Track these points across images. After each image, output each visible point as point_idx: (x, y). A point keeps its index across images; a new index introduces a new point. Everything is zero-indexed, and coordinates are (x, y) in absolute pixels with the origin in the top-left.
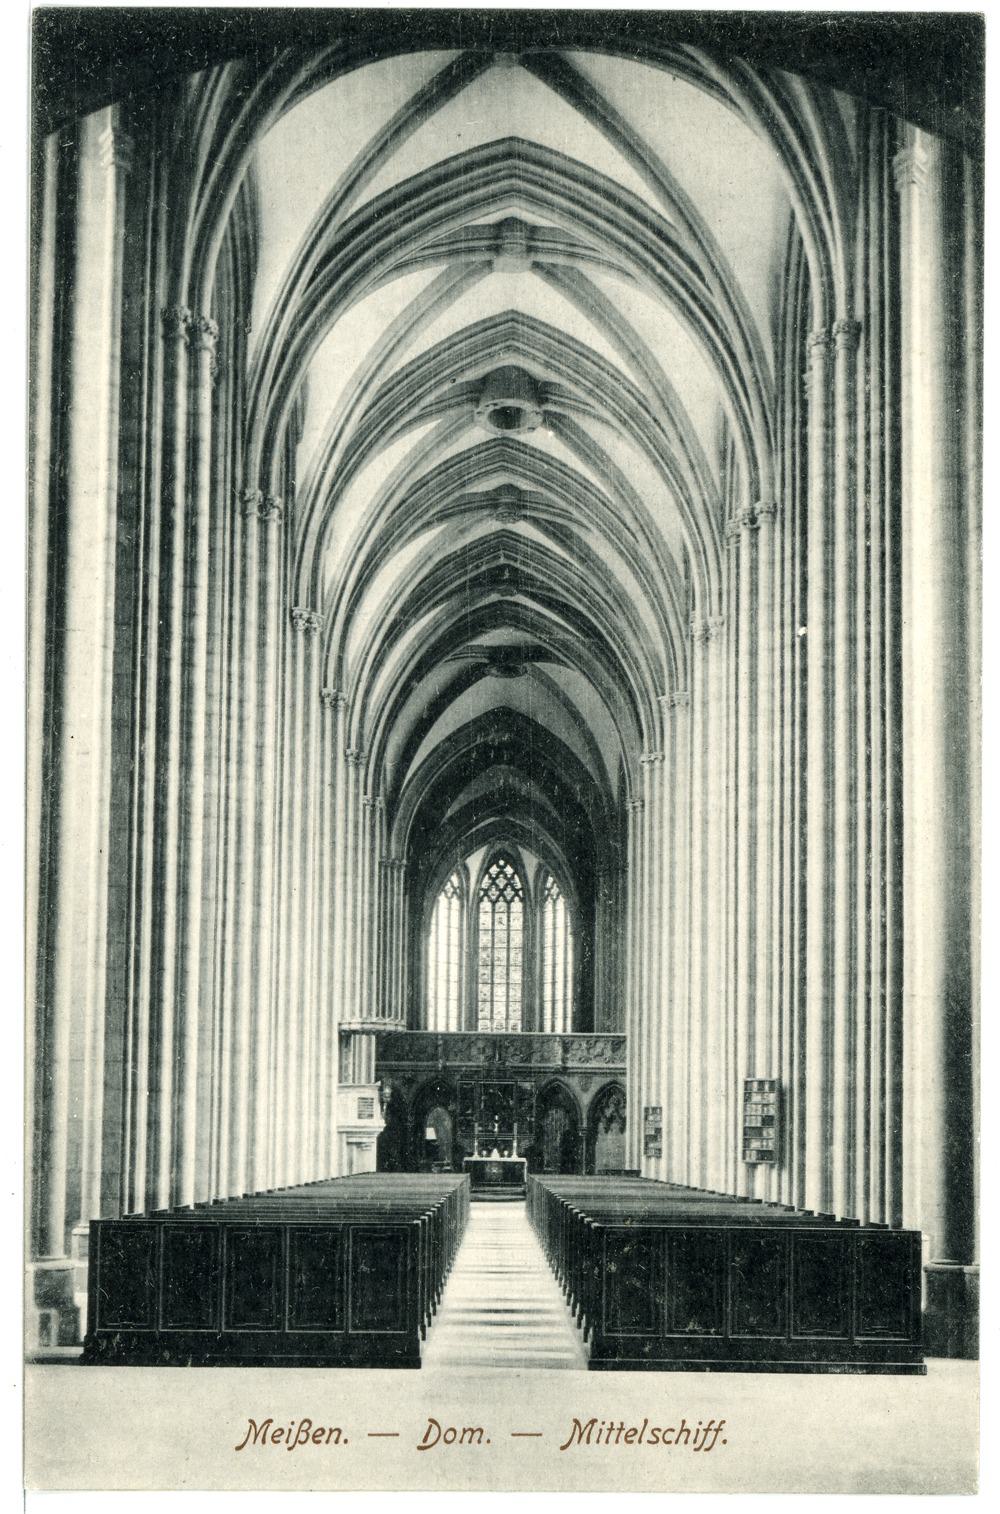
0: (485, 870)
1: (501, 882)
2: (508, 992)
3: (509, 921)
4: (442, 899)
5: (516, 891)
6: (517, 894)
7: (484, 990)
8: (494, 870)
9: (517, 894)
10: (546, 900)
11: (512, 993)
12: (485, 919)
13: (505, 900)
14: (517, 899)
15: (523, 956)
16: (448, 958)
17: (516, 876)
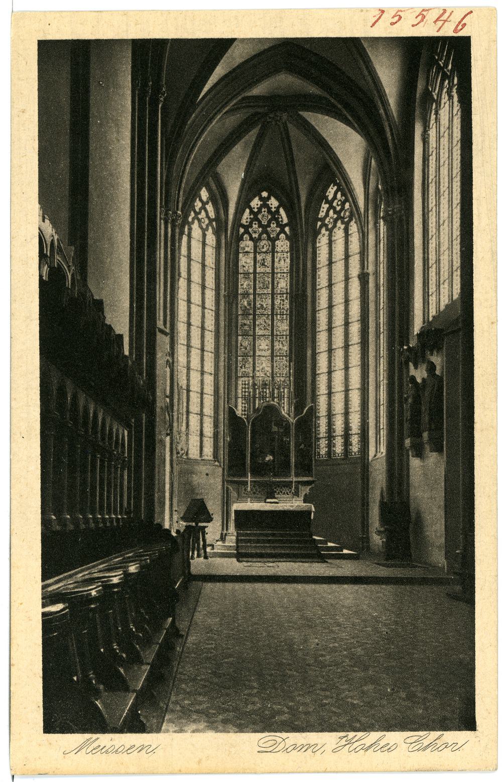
0: (244, 203)
1: (264, 217)
2: (273, 346)
3: (273, 262)
4: (196, 232)
5: (282, 227)
6: (283, 231)
7: (244, 342)
8: (256, 203)
9: (283, 231)
10: (319, 233)
11: (277, 346)
12: (246, 262)
13: (269, 238)
14: (282, 236)
15: (291, 303)
16: (203, 322)
17: (282, 211)
